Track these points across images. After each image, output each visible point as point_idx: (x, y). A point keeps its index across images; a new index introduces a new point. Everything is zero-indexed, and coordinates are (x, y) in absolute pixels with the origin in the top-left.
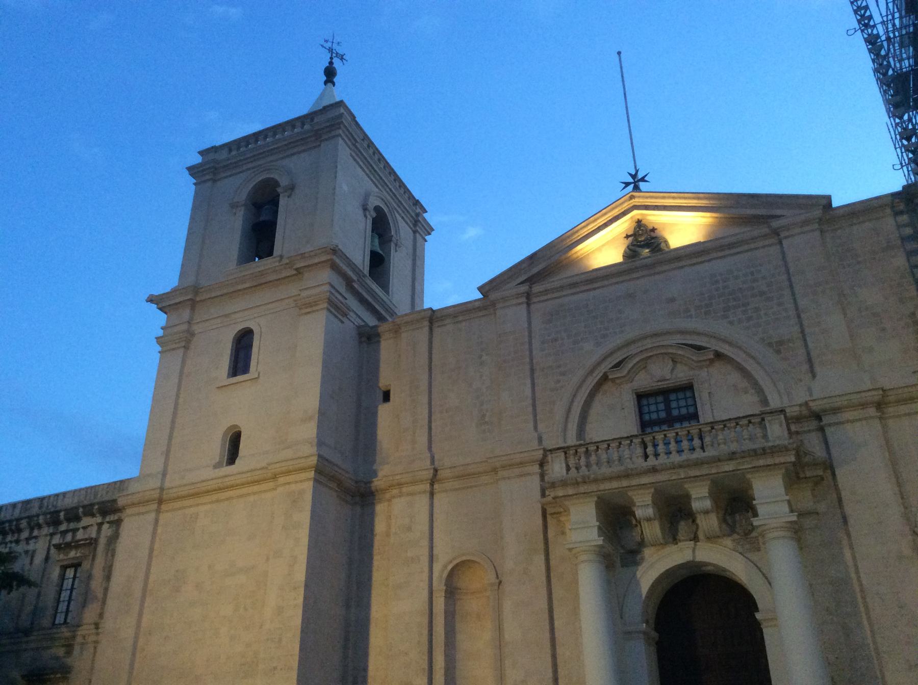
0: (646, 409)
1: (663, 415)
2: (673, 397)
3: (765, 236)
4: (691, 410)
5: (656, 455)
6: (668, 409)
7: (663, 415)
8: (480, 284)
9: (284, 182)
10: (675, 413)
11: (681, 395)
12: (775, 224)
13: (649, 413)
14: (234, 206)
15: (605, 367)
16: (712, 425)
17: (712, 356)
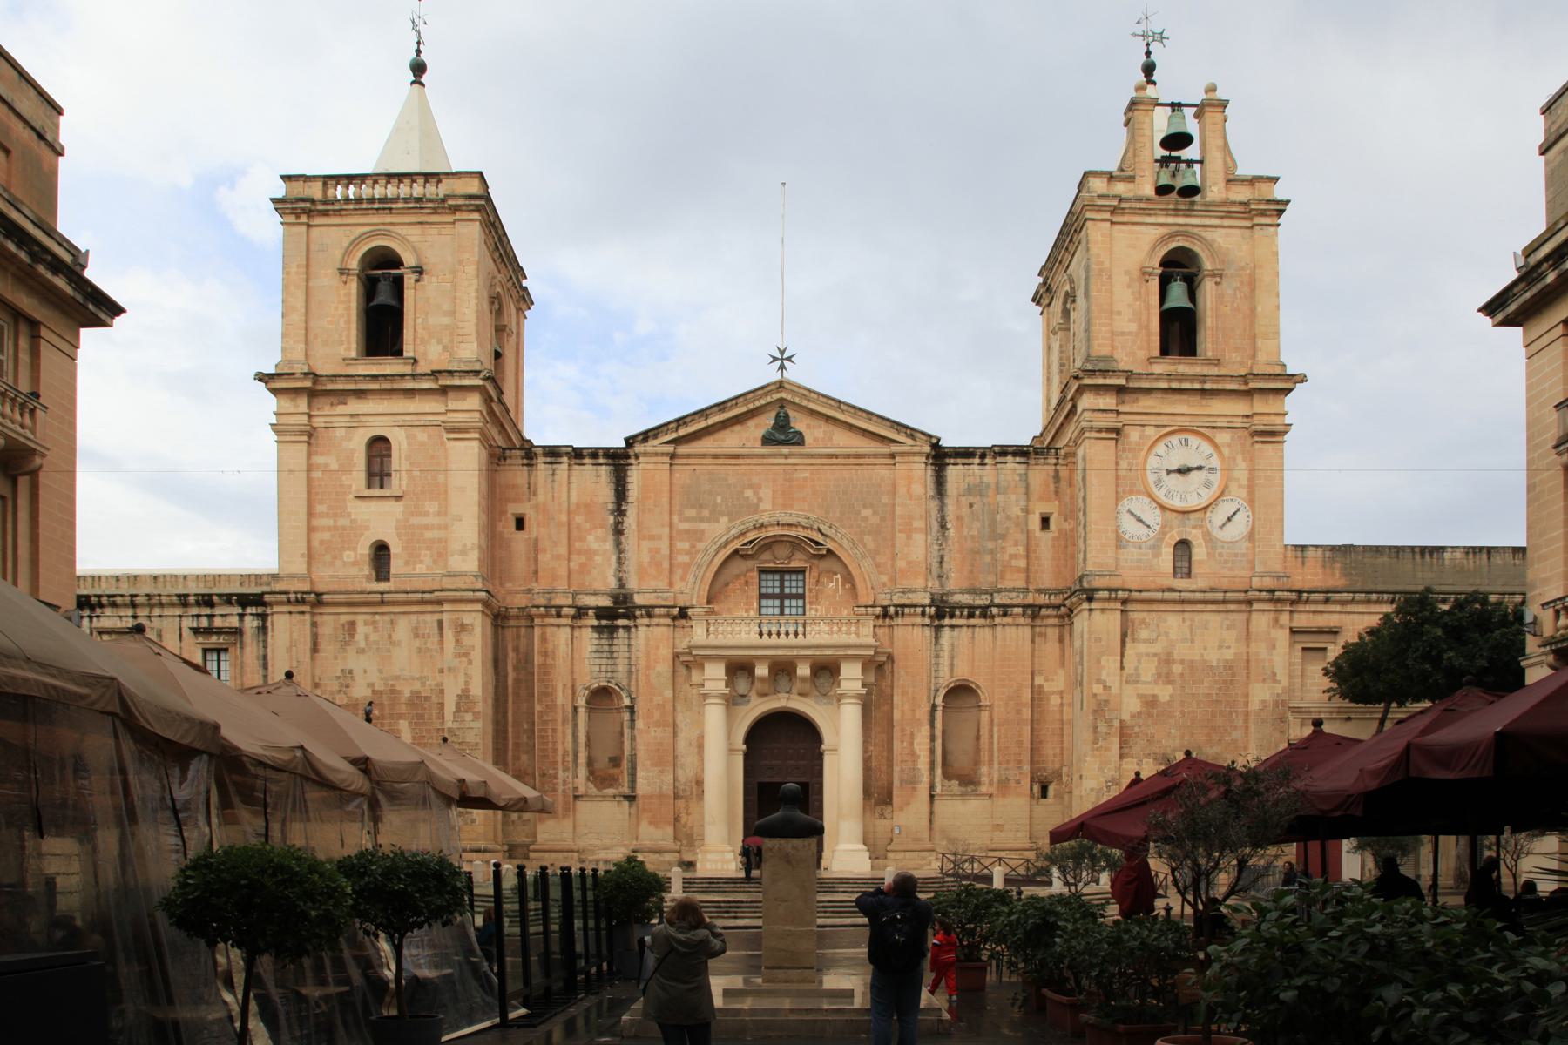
0: (764, 584)
1: (777, 591)
2: (787, 577)
3: (883, 456)
4: (800, 591)
5: (770, 634)
6: (782, 587)
7: (777, 591)
8: (628, 435)
9: (409, 259)
10: (787, 591)
11: (794, 577)
12: (894, 448)
13: (767, 587)
14: (343, 272)
15: (736, 545)
16: (813, 619)
17: (825, 552)
